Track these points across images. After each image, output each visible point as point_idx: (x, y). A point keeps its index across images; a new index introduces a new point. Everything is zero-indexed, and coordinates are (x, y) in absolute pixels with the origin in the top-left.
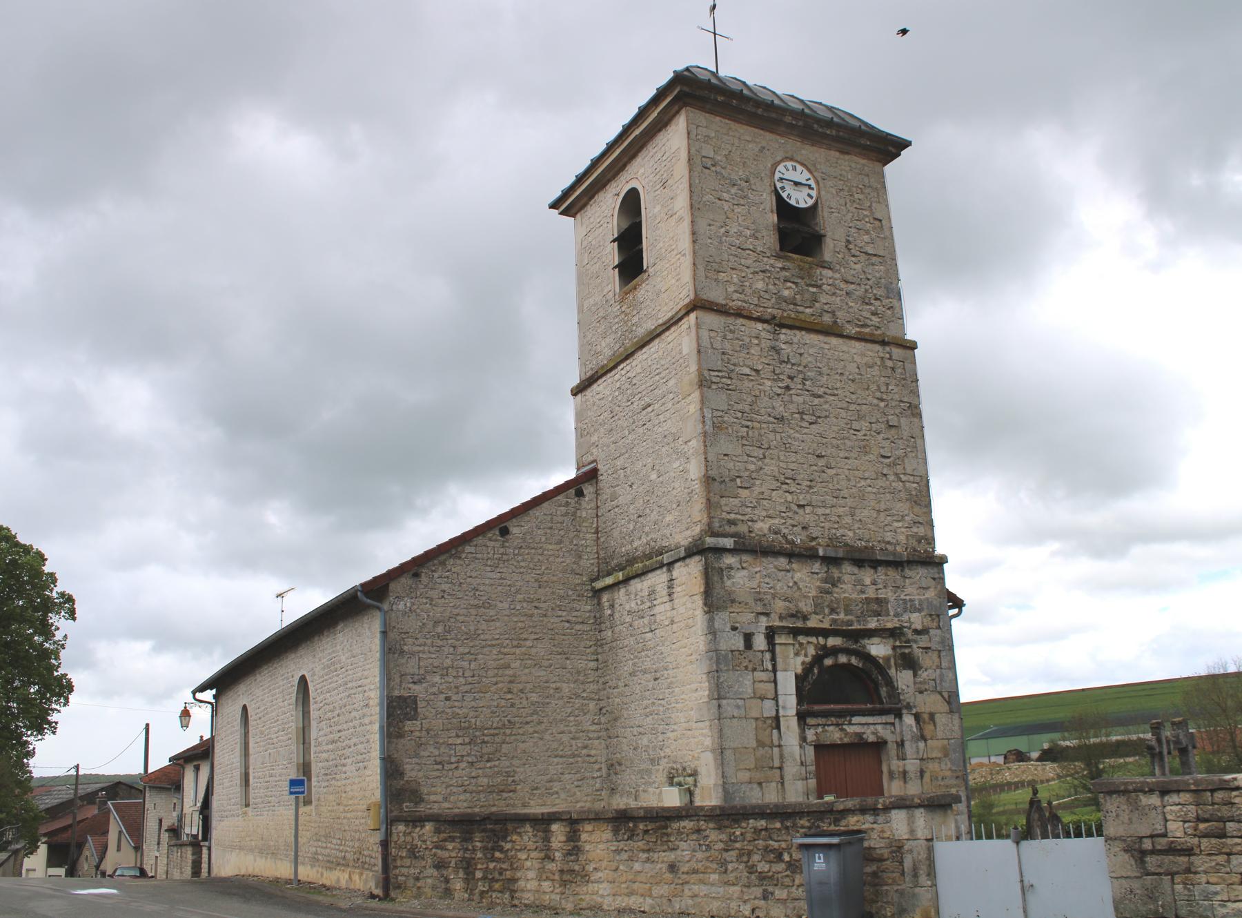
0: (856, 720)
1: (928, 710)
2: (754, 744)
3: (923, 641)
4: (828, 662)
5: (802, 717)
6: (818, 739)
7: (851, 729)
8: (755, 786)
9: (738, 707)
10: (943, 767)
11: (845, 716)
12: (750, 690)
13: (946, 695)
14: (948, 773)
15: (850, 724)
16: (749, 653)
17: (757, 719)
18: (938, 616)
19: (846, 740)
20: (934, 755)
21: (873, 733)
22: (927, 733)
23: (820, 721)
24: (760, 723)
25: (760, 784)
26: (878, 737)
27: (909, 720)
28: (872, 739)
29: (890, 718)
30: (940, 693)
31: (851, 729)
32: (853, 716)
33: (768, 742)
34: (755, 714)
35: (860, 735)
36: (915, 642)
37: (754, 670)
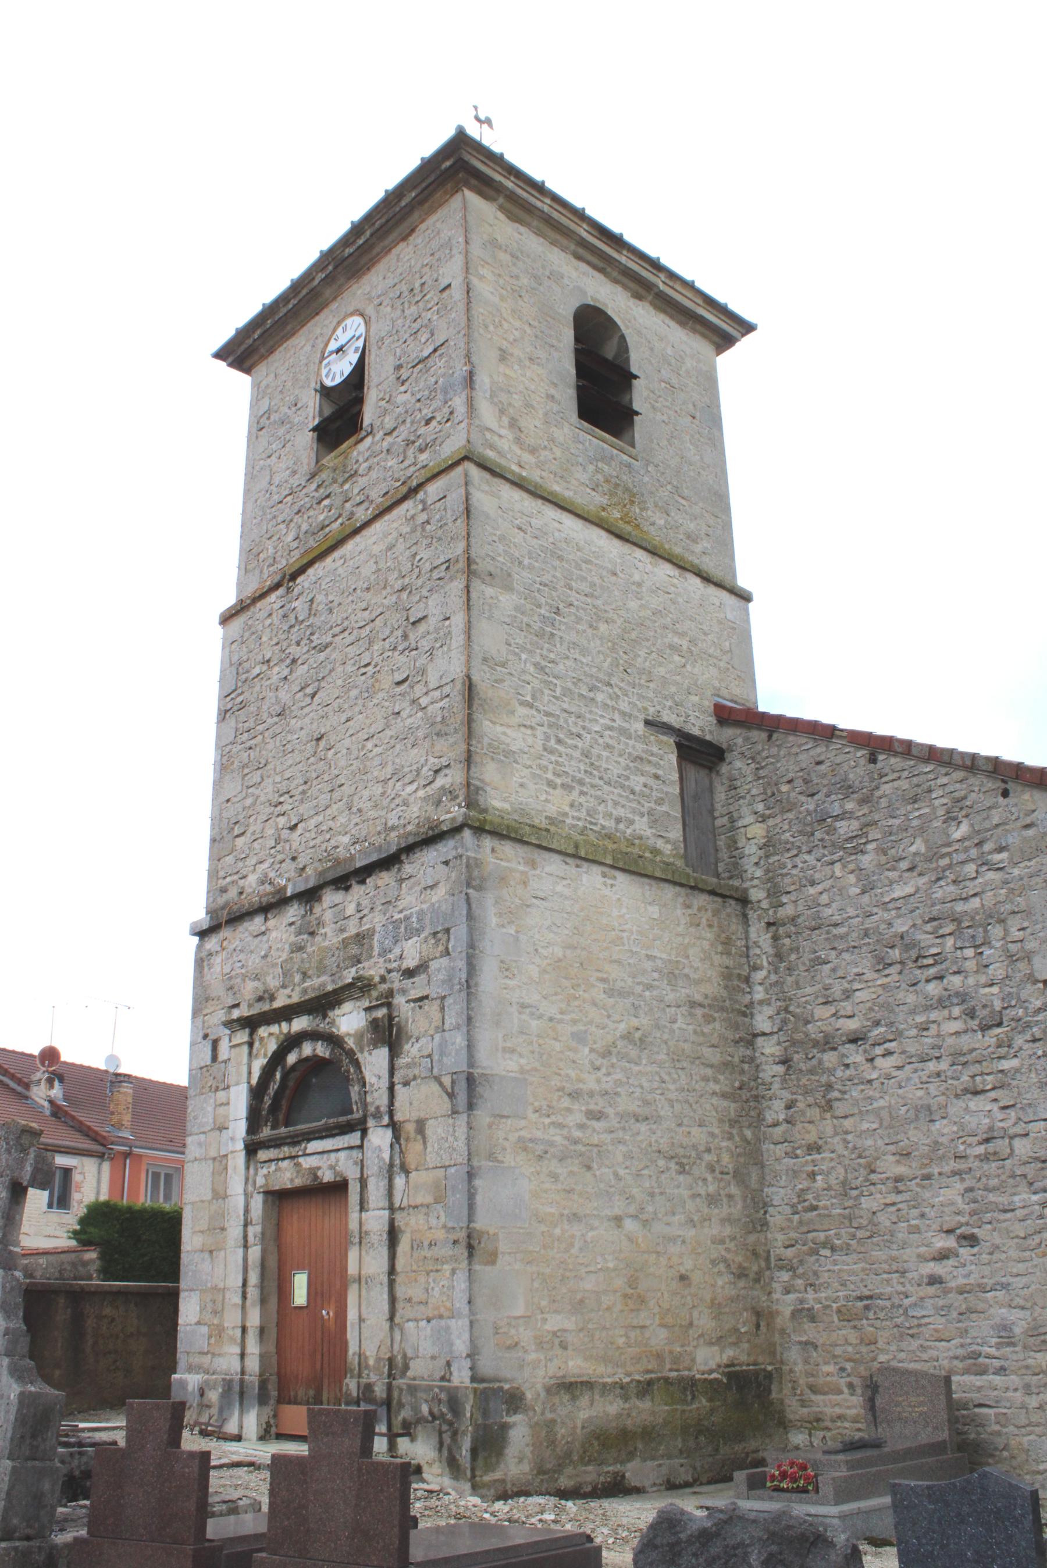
0: (314, 1146)
1: (415, 1116)
2: (208, 1196)
3: (417, 987)
4: (292, 1059)
5: (251, 1149)
6: (266, 1185)
7: (306, 1163)
8: (207, 1255)
9: (200, 1144)
10: (433, 1222)
11: (298, 1143)
12: (211, 1121)
13: (447, 1081)
14: (440, 1235)
15: (305, 1155)
16: (216, 1065)
17: (214, 1159)
18: (447, 931)
19: (298, 1182)
20: (419, 1200)
21: (332, 1167)
22: (411, 1160)
23: (272, 1153)
24: (217, 1163)
25: (211, 1252)
26: (336, 1174)
27: (379, 1138)
28: (327, 1177)
29: (354, 1138)
30: (438, 1079)
31: (306, 1163)
32: (309, 1140)
33: (222, 1192)
34: (213, 1153)
35: (313, 1172)
36: (404, 991)
37: (217, 1089)
